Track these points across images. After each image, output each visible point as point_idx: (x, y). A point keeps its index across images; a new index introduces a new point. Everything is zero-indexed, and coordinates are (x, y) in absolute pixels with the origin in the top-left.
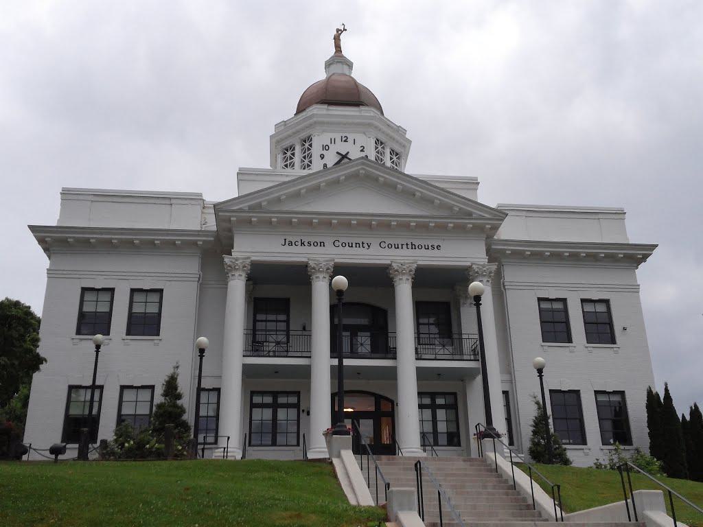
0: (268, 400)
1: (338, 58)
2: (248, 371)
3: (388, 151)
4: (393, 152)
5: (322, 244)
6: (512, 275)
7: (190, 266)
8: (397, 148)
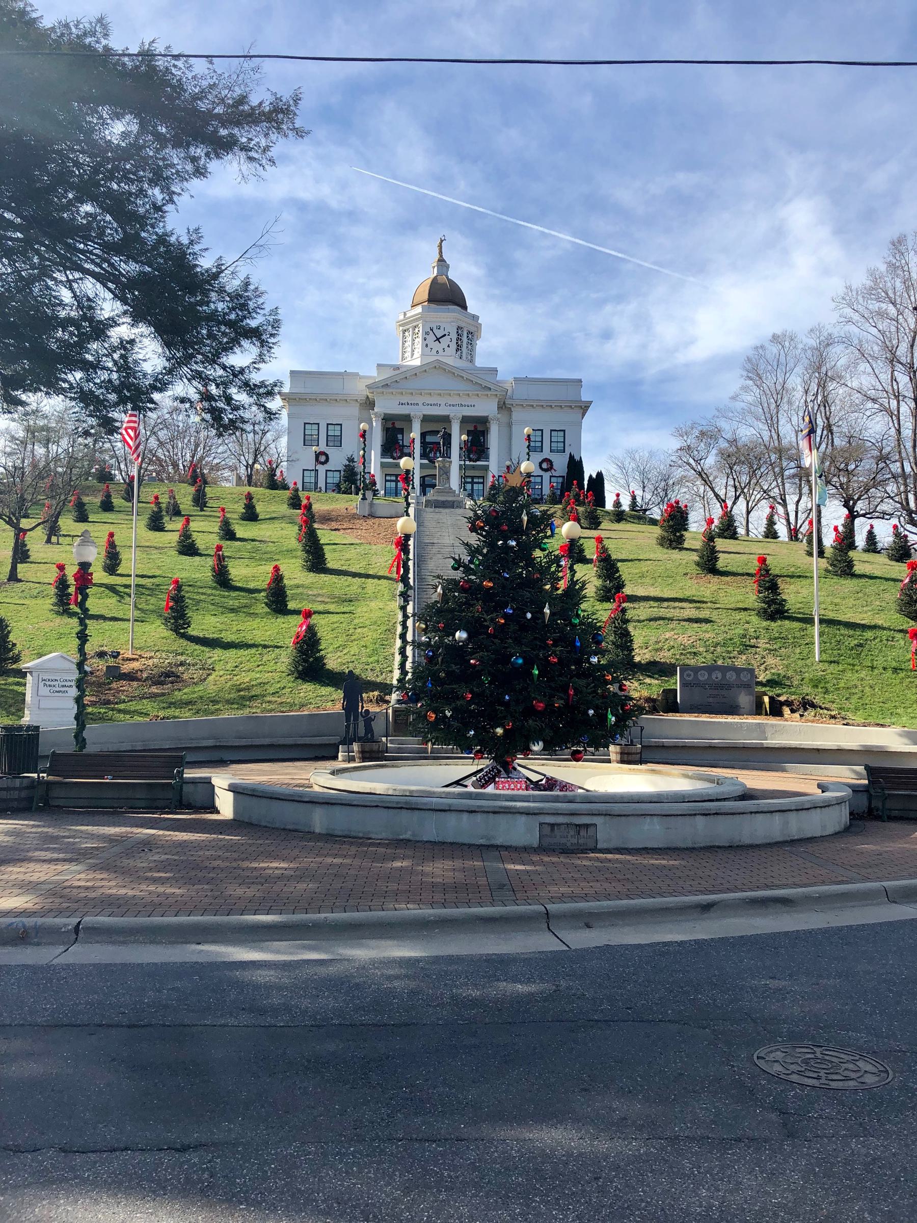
0: (394, 478)
1: (442, 262)
2: (383, 465)
3: (465, 335)
4: (469, 333)
5: (417, 404)
6: (517, 415)
7: (355, 410)
8: (472, 329)
